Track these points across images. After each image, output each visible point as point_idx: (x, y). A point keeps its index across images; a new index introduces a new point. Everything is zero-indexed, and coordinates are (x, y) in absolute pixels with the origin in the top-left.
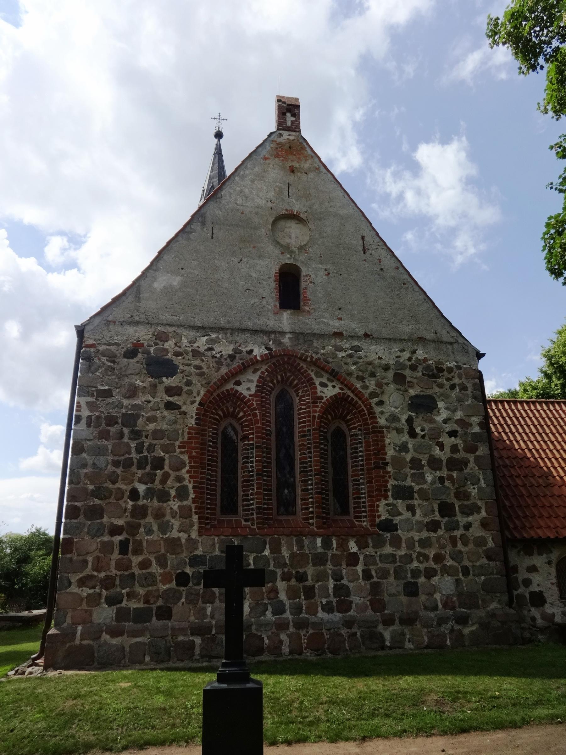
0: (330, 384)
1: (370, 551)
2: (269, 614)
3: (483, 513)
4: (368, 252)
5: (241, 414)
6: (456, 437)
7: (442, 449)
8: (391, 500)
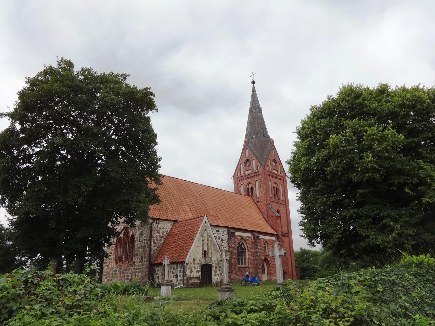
1: (132, 268)
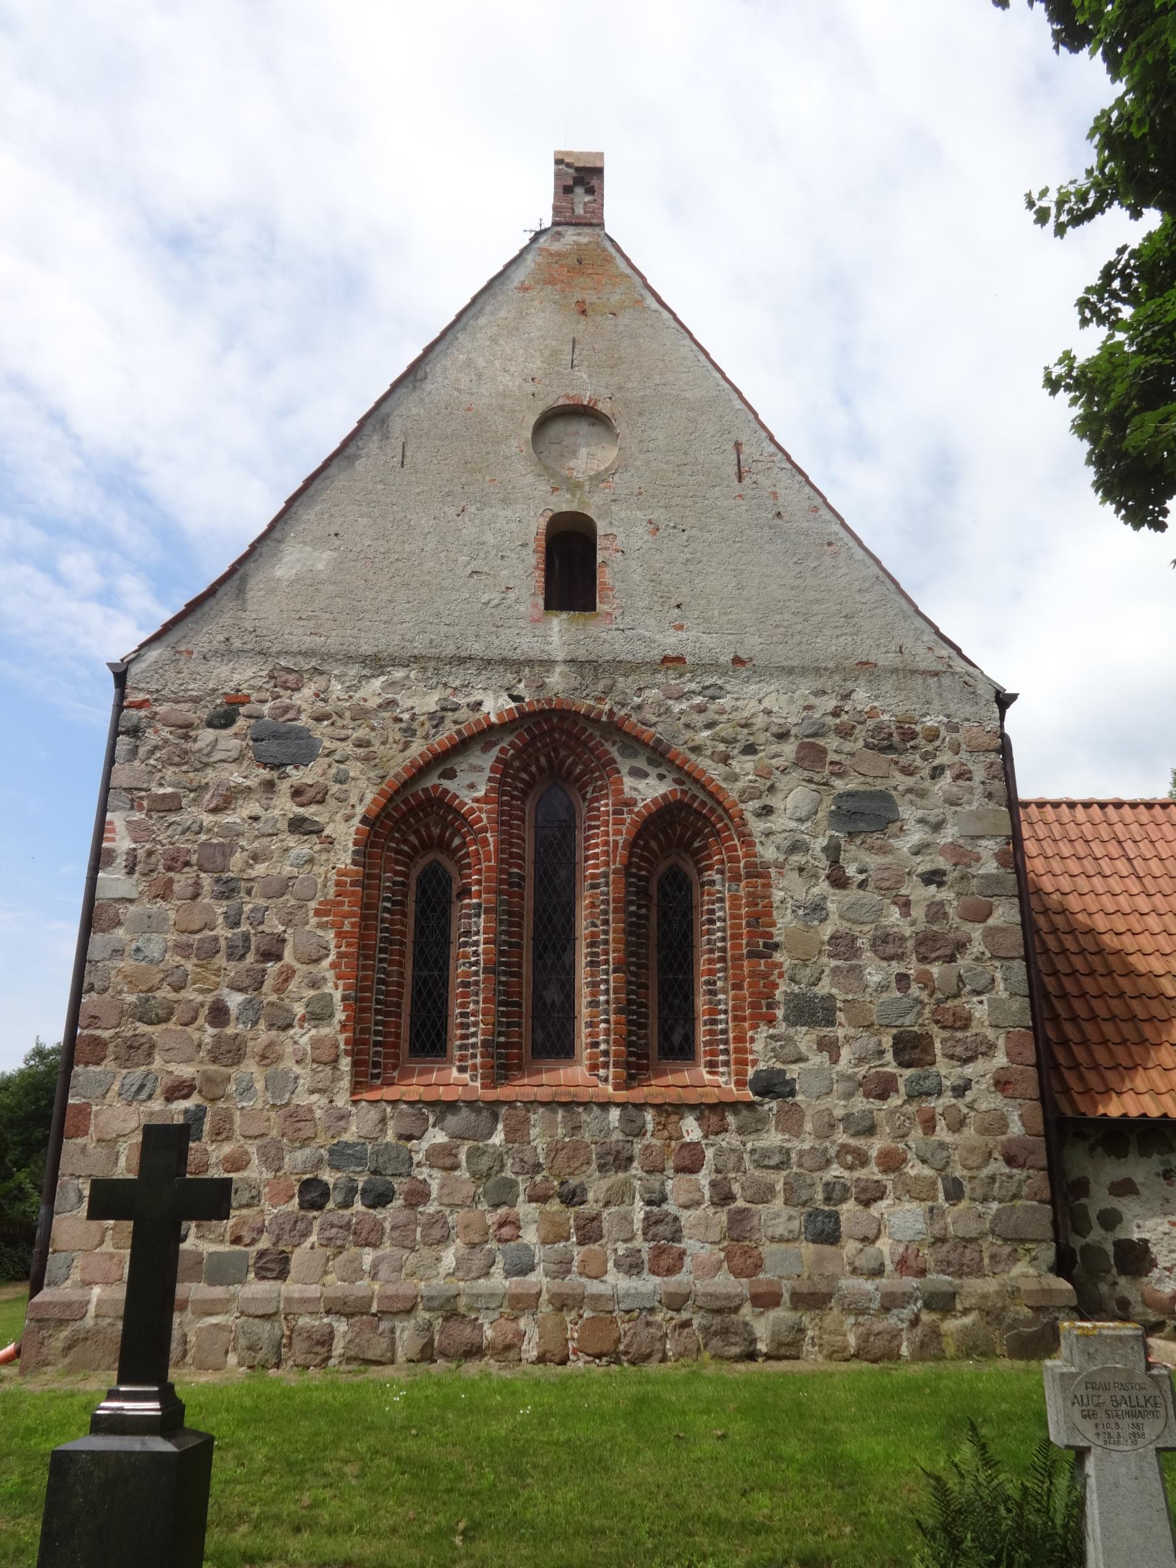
0: (653, 772)
1: (731, 1139)
2: (497, 1270)
3: (1000, 1060)
4: (747, 481)
5: (457, 841)
6: (940, 884)
7: (906, 913)
8: (781, 1028)
